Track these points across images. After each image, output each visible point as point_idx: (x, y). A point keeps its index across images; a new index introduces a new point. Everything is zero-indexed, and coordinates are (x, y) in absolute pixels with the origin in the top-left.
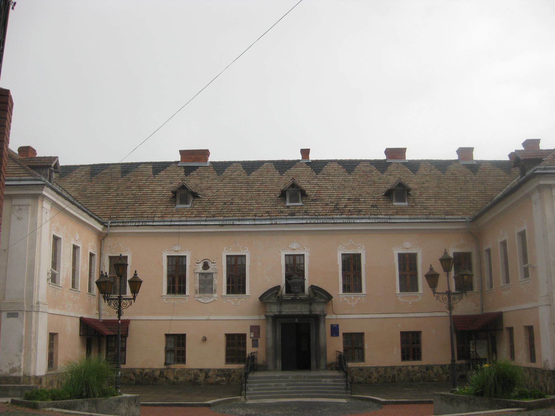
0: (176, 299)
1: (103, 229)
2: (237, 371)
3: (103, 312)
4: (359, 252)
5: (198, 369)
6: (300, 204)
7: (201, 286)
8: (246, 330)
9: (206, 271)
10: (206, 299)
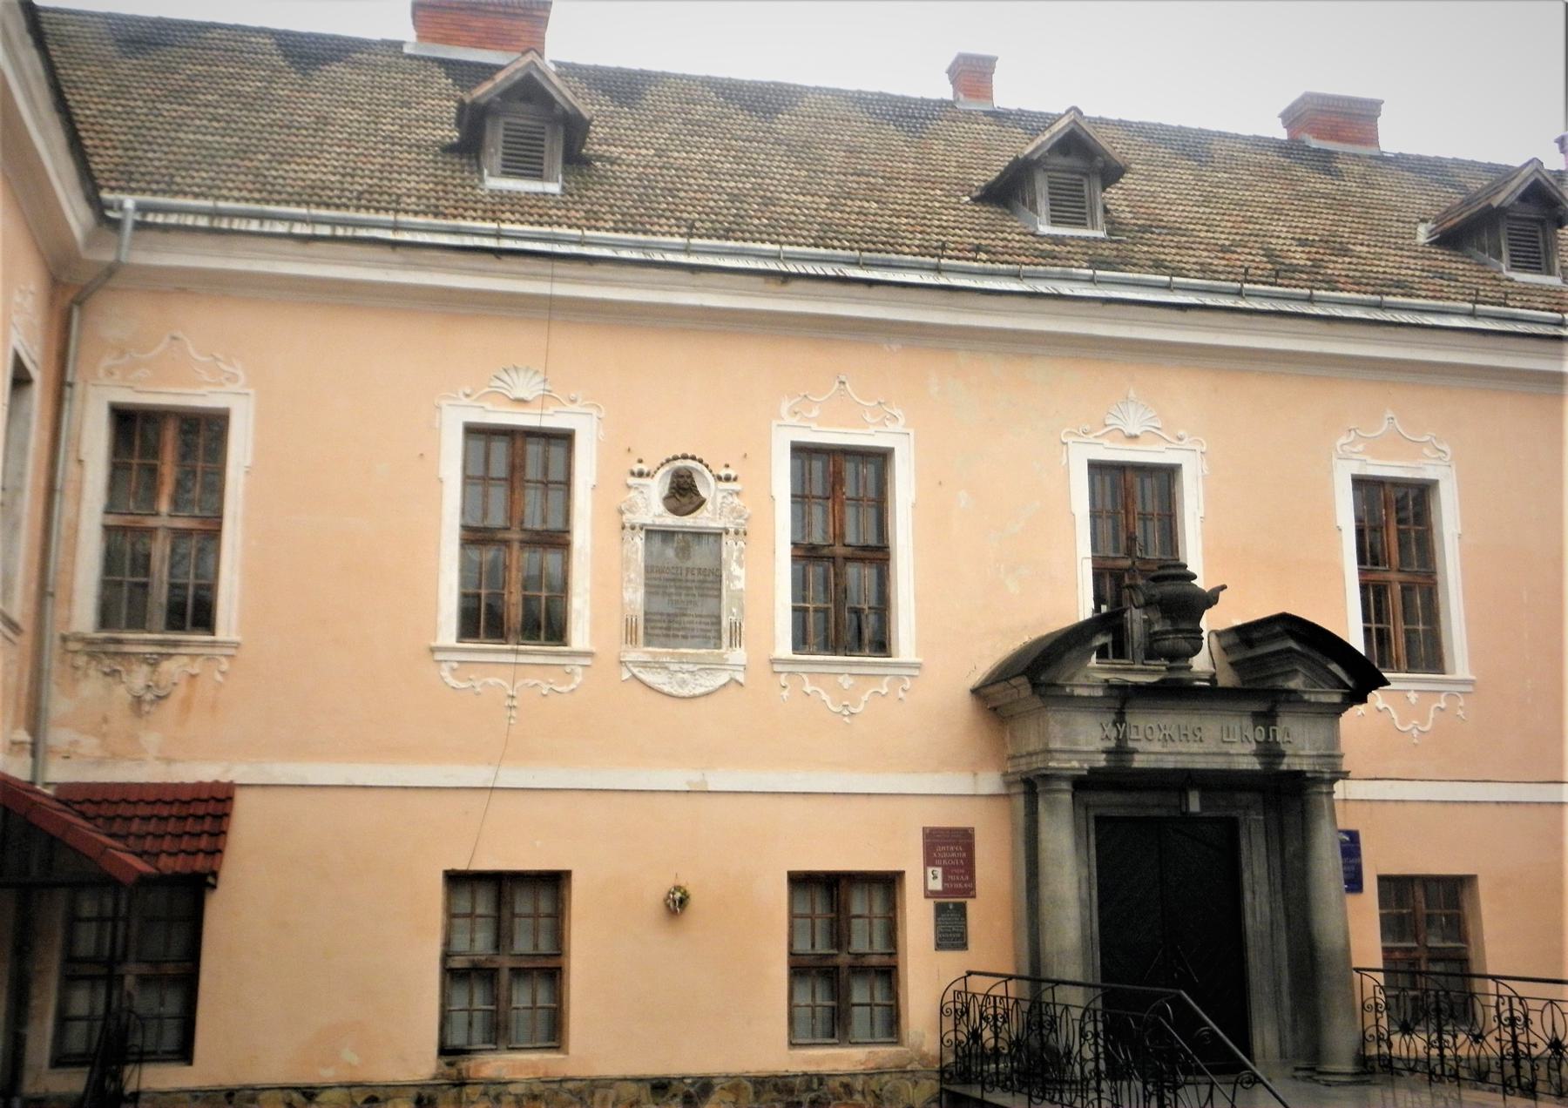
0: (507, 667)
1: (91, 240)
2: (858, 1084)
3: (58, 737)
4: (1428, 474)
5: (638, 1080)
6: (1101, 234)
7: (662, 605)
8: (902, 852)
9: (688, 522)
10: (682, 672)
